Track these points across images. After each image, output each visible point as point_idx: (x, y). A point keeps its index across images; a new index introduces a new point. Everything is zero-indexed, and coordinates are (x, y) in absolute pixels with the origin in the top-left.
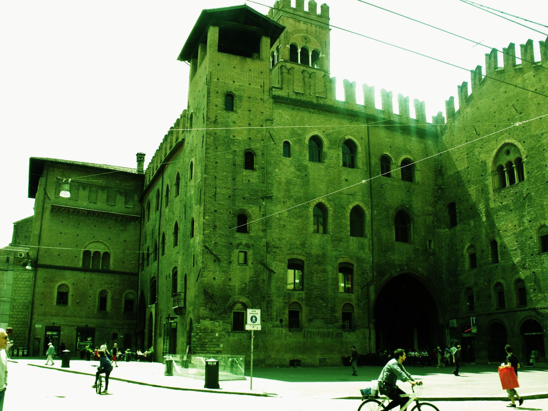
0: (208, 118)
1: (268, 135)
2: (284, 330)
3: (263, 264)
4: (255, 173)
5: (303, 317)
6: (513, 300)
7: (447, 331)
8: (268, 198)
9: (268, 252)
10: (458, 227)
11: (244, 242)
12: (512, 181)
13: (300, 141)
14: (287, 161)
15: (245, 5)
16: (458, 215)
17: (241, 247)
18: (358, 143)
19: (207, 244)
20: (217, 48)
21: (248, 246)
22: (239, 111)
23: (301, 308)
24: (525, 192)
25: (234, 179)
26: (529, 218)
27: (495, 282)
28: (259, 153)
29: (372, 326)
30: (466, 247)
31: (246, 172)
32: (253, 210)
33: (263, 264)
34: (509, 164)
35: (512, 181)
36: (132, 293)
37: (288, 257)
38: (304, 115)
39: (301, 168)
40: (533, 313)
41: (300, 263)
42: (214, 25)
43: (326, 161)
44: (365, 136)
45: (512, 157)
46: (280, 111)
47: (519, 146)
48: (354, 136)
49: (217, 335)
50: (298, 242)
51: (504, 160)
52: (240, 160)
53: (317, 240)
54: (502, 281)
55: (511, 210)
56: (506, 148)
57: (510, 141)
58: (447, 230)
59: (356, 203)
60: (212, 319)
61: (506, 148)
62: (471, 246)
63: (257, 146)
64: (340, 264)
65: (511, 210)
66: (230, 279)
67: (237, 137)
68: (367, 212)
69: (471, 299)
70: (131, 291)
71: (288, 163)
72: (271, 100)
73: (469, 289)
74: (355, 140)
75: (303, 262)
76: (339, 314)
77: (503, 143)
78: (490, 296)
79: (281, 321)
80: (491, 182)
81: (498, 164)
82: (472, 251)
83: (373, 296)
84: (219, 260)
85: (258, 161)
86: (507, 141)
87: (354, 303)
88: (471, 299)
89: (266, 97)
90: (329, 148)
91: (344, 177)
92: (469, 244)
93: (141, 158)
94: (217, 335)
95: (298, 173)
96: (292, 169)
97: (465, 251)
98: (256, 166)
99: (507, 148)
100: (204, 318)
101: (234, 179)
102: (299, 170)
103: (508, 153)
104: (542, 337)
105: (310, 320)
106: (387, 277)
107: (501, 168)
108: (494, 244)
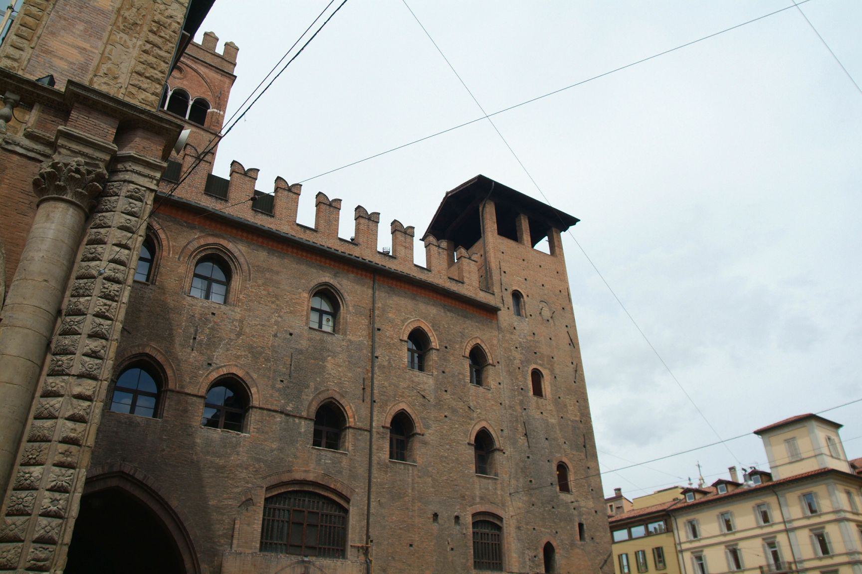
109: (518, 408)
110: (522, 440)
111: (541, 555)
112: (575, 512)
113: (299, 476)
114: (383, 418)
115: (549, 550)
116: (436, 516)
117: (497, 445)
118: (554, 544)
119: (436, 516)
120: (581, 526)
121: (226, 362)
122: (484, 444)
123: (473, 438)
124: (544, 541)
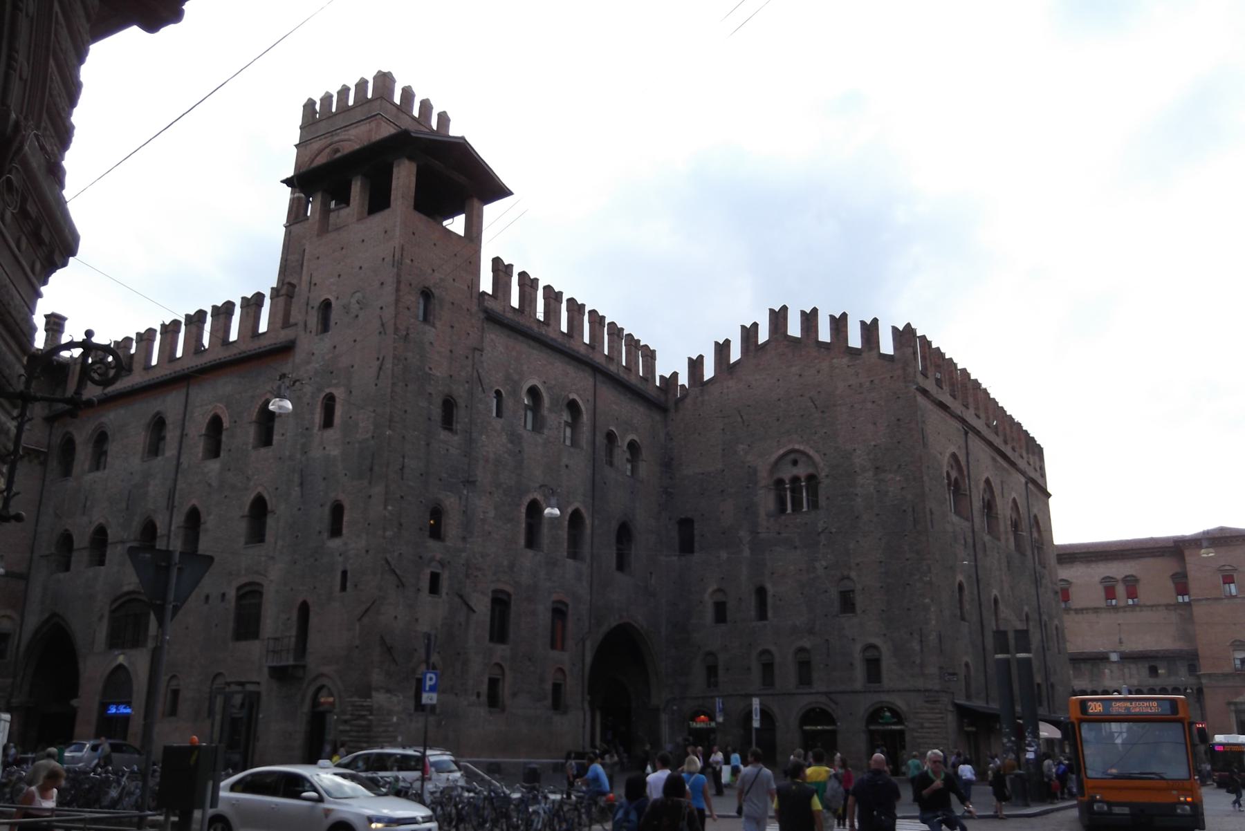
0: (396, 329)
1: (475, 374)
2: (483, 711)
3: (461, 597)
4: (456, 438)
5: (506, 689)
6: (787, 676)
7: (664, 717)
8: (470, 483)
9: (467, 576)
10: (697, 557)
11: (438, 556)
12: (797, 504)
13: (515, 393)
14: (498, 424)
15: (463, 138)
16: (697, 539)
17: (434, 564)
18: (583, 408)
19: (388, 556)
20: (412, 202)
21: (442, 564)
22: (438, 324)
23: (503, 674)
24: (821, 526)
25: (428, 445)
26: (824, 563)
27: (760, 648)
28: (461, 403)
29: (586, 706)
30: (710, 590)
31: (443, 435)
32: (451, 502)
33: (461, 597)
34: (795, 479)
35: (797, 504)
36: (9, 617)
37: (493, 586)
38: (523, 348)
39: (515, 438)
40: (823, 699)
41: (505, 597)
42: (410, 158)
43: (546, 431)
44: (591, 399)
45: (801, 471)
46: (493, 336)
47: (817, 457)
48: (579, 396)
49: (395, 719)
50: (505, 563)
51: (787, 473)
52: (437, 412)
53: (529, 559)
54: (773, 649)
55: (795, 548)
56: (792, 456)
57: (802, 448)
58: (675, 558)
59: (576, 505)
60: (388, 691)
61: (792, 456)
62: (719, 590)
63: (460, 392)
64: (554, 602)
65: (795, 548)
66: (417, 620)
67: (434, 372)
68: (588, 521)
69: (712, 671)
70: (9, 612)
71: (499, 427)
72: (482, 316)
73: (710, 653)
74: (580, 402)
75: (509, 595)
76: (548, 687)
77: (790, 447)
78: (749, 669)
79: (478, 695)
80: (766, 501)
81: (776, 476)
82: (720, 597)
83: (589, 659)
84: (403, 585)
85: (461, 415)
86: (797, 447)
87: (566, 669)
88: (712, 671)
89: (475, 309)
90: (550, 410)
91: (565, 461)
92: (715, 587)
93: (55, 323)
94: (395, 719)
95: (510, 446)
96: (504, 439)
97: (707, 597)
98: (458, 427)
99: (795, 457)
100: (377, 690)
101: (428, 445)
102: (512, 442)
103: (795, 463)
104: (834, 733)
105: (514, 695)
106: (605, 629)
107: (780, 482)
108: (761, 592)
109: (298, 456)
110: (296, 491)
111: (295, 615)
112: (340, 559)
113: (126, 589)
114: (179, 519)
115: (304, 610)
116: (207, 597)
117: (269, 507)
118: (310, 601)
119: (207, 597)
120: (344, 573)
121: (97, 518)
122: (260, 508)
123: (247, 508)
124: (300, 600)
